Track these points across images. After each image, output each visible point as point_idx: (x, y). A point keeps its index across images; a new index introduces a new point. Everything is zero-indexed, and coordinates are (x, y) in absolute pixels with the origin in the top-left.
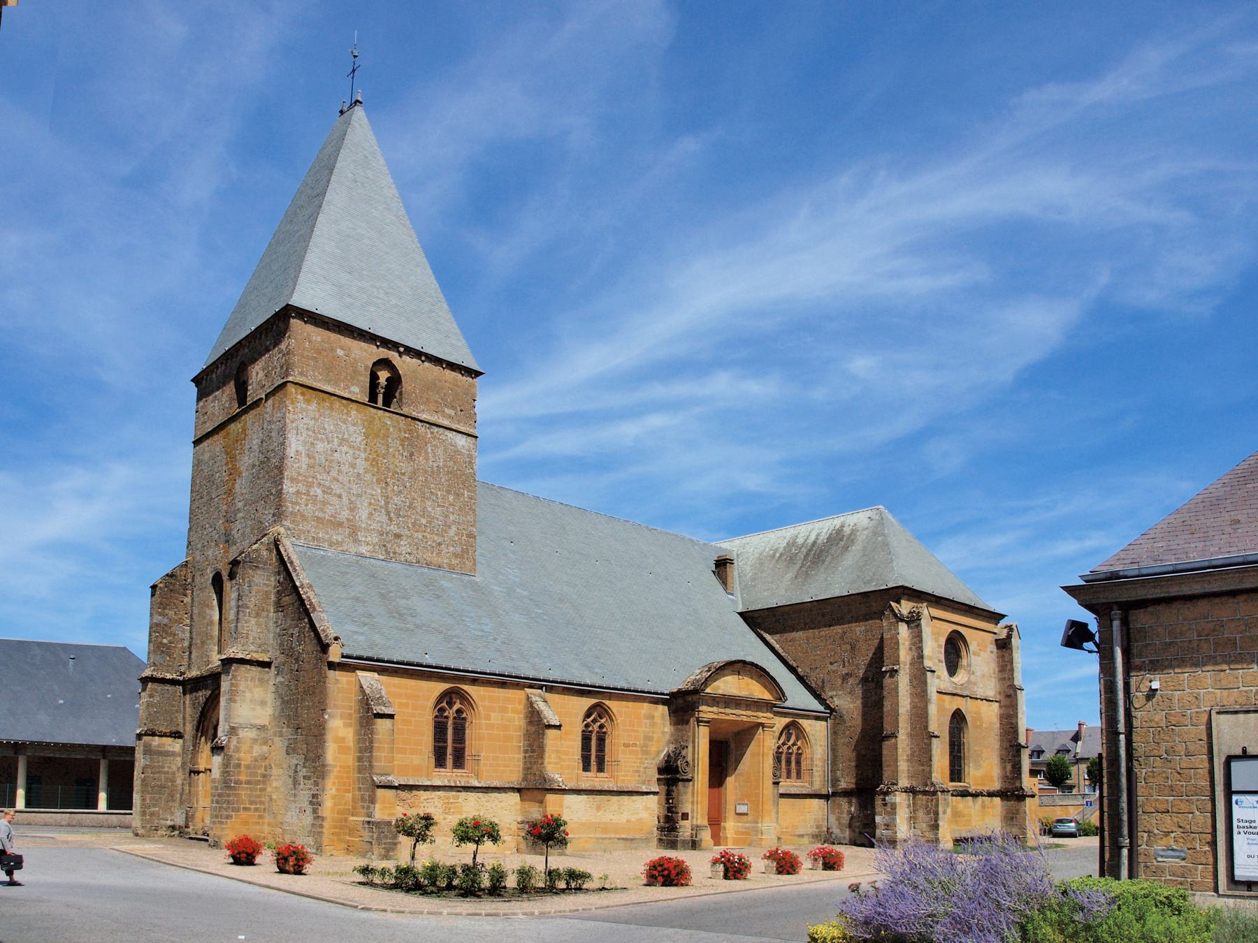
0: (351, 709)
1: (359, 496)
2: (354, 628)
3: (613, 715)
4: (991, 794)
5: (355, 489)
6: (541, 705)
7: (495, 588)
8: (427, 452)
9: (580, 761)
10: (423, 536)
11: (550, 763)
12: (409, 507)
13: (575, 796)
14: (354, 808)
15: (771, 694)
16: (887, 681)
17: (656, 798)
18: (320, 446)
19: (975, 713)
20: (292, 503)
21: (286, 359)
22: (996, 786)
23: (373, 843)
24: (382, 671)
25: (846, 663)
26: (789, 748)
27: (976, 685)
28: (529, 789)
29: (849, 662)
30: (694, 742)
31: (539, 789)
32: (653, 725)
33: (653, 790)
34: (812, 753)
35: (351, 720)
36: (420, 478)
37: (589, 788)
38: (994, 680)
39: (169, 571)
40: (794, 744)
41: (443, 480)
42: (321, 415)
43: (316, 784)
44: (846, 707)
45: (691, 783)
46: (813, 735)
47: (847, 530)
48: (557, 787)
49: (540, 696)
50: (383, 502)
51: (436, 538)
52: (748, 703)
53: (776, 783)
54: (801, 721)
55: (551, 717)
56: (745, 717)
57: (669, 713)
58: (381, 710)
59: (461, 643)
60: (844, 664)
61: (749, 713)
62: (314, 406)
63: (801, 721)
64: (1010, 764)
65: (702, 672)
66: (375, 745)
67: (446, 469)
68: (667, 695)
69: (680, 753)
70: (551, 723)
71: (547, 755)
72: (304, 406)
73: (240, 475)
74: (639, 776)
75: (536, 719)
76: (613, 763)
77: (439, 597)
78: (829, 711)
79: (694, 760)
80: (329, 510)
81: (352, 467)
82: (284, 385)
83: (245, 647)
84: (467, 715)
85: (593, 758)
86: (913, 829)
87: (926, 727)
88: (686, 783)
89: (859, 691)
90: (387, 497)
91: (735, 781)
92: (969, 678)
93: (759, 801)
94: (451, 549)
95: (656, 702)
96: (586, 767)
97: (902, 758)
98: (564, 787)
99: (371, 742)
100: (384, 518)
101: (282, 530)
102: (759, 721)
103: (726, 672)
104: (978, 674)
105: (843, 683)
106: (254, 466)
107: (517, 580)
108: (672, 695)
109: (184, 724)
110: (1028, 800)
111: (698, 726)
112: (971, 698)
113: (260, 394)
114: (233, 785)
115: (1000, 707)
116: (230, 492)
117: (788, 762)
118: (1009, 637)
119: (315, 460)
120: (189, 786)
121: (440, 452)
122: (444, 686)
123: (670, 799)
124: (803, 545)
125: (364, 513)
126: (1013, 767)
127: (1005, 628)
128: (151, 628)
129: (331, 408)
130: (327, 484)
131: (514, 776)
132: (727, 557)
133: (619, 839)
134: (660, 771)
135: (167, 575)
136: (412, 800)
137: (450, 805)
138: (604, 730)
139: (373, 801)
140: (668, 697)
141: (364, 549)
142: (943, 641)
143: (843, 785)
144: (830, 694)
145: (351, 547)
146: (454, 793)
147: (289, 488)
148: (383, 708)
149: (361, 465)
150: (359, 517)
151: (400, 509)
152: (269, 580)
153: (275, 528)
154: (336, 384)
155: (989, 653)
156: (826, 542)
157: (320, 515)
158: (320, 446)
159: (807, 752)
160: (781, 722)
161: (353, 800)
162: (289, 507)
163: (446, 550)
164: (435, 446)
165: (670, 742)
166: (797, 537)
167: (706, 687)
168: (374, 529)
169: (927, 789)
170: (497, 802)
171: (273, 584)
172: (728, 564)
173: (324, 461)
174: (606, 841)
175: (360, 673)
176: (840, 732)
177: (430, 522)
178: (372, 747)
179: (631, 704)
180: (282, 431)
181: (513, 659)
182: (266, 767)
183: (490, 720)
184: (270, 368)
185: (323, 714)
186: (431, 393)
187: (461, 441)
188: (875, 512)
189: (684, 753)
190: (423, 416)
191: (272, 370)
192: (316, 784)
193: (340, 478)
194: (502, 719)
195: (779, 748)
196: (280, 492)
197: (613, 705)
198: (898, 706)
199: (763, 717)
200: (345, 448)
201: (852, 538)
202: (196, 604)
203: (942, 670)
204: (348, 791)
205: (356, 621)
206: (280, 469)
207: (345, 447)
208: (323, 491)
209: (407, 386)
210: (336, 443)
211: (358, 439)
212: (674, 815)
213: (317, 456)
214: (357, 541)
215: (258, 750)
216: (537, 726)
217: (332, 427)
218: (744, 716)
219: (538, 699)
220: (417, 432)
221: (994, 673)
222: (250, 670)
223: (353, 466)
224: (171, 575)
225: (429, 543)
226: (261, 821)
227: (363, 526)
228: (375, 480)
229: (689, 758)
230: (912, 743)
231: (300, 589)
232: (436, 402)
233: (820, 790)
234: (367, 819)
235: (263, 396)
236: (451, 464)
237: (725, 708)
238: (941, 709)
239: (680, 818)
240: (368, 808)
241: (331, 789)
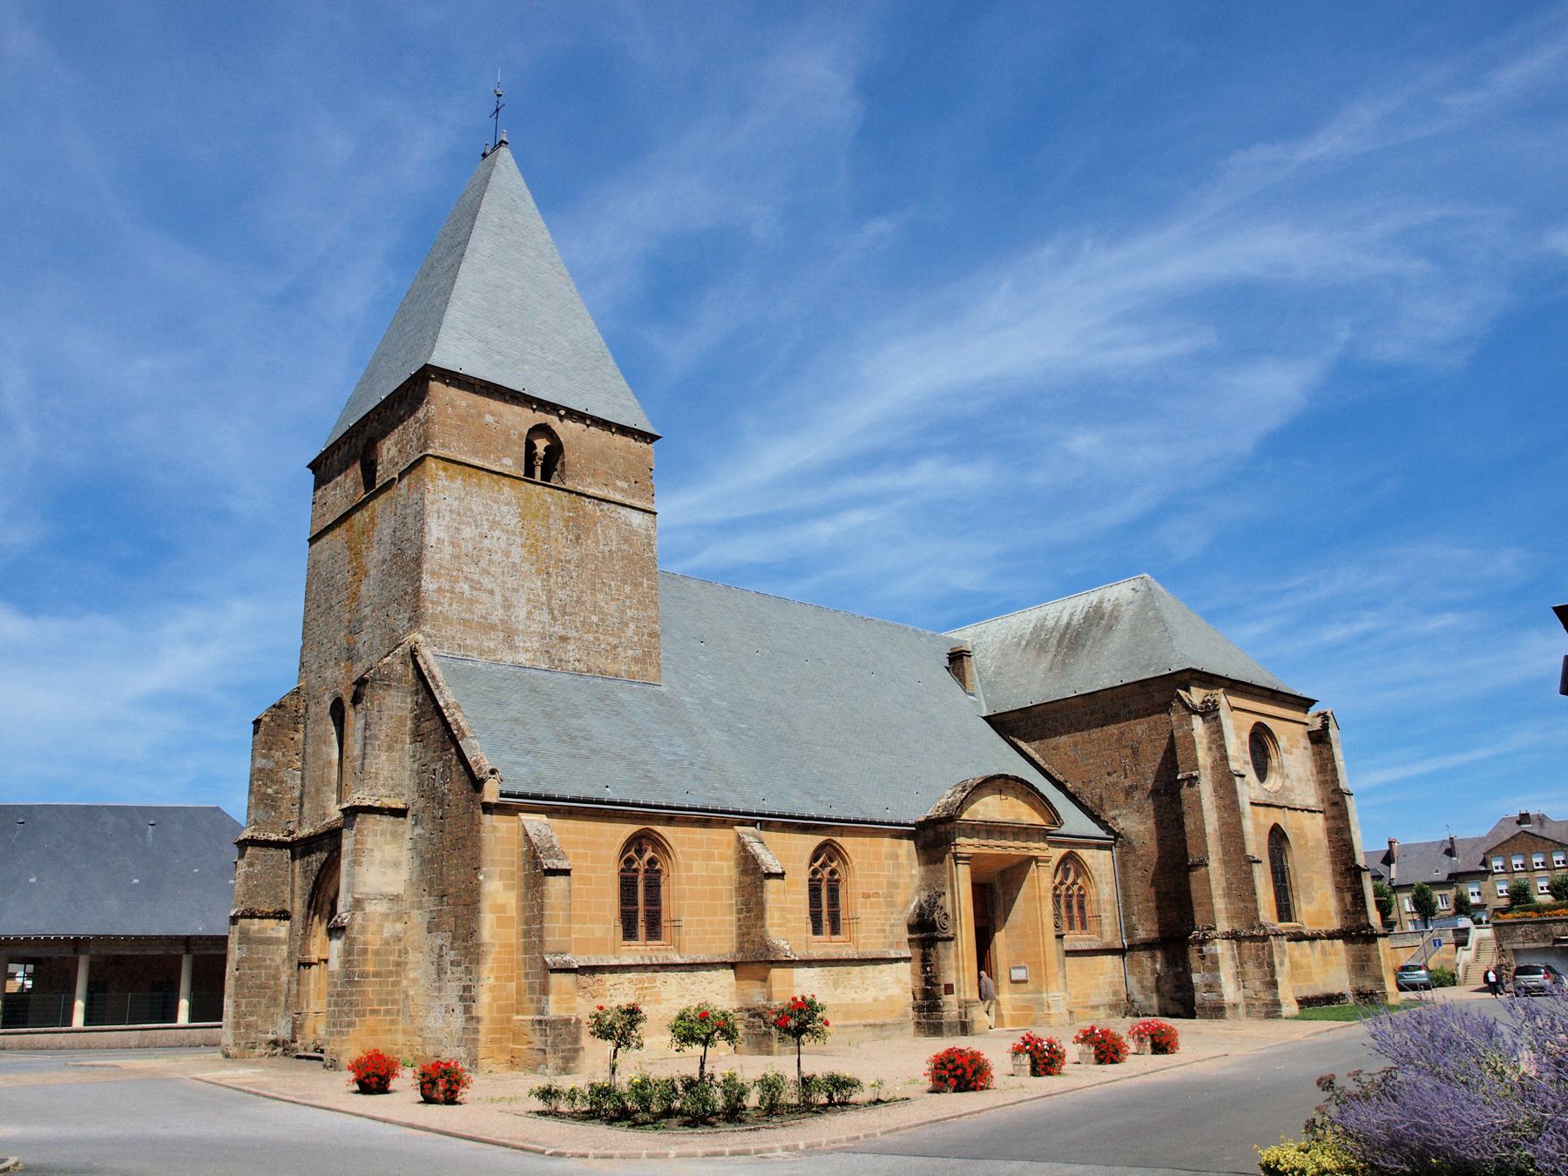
0: (513, 866)
1: (515, 590)
2: (513, 757)
3: (846, 856)
4: (1331, 936)
5: (511, 582)
6: (757, 848)
7: (687, 699)
8: (596, 535)
9: (809, 920)
10: (595, 638)
11: (772, 925)
12: (577, 602)
13: (806, 969)
14: (519, 1002)
15: (1043, 817)
16: (1185, 791)
17: (908, 965)
18: (467, 532)
19: (1297, 829)
20: (432, 602)
21: (424, 430)
22: (1335, 924)
23: (547, 1051)
24: (551, 812)
26: (1068, 888)
27: (1292, 791)
28: (747, 963)
29: (1131, 769)
30: (952, 886)
31: (760, 962)
32: (898, 866)
33: (904, 955)
34: (1098, 894)
35: (513, 880)
36: (589, 566)
37: (823, 957)
38: (1312, 784)
39: (276, 701)
40: (1074, 883)
41: (616, 567)
42: (467, 494)
43: (468, 971)
45: (953, 942)
46: (1096, 870)
47: (1107, 606)
48: (784, 959)
49: (754, 835)
50: (544, 597)
51: (611, 639)
52: (1016, 830)
53: (1060, 937)
54: (1079, 851)
55: (771, 862)
56: (1013, 849)
57: (917, 849)
58: (553, 864)
59: (649, 771)
62: (458, 483)
63: (1079, 851)
64: (1350, 894)
65: (954, 792)
66: (546, 913)
67: (620, 554)
68: (911, 825)
69: (935, 903)
71: (768, 914)
72: (447, 483)
73: (366, 574)
74: (885, 937)
76: (851, 922)
77: (617, 713)
78: (1112, 837)
79: (954, 910)
80: (479, 610)
81: (506, 555)
82: (423, 459)
83: (374, 791)
84: (662, 865)
85: (825, 916)
86: (1242, 989)
87: (1243, 850)
88: (948, 943)
89: (1149, 806)
90: (550, 591)
91: (1007, 937)
92: (1283, 783)
93: (1040, 963)
94: (630, 652)
96: (817, 930)
97: (1217, 893)
98: (792, 957)
99: (542, 909)
100: (546, 617)
101: (420, 637)
102: (1031, 853)
103: (985, 791)
104: (1293, 777)
105: (1126, 798)
106: (384, 561)
107: (712, 688)
108: (919, 825)
109: (292, 900)
110: (1380, 941)
111: (956, 864)
112: (1289, 808)
113: (392, 473)
114: (356, 979)
115: (1326, 819)
116: (354, 596)
117: (1069, 907)
118: (1325, 727)
119: (460, 548)
120: (298, 984)
121: (612, 532)
122: (632, 828)
124: (1054, 629)
125: (521, 613)
126: (1355, 897)
127: (1318, 716)
128: (252, 775)
129: (479, 485)
130: (476, 577)
131: (724, 945)
132: (963, 648)
133: (865, 1026)
134: (912, 928)
135: (274, 706)
136: (596, 987)
137: (645, 991)
138: (836, 877)
139: (545, 990)
140: (914, 829)
141: (522, 658)
142: (1246, 736)
143: (1141, 934)
144: (1112, 813)
145: (506, 656)
146: (649, 974)
147: (429, 584)
148: (556, 861)
149: (517, 553)
150: (516, 617)
151: (566, 605)
152: (406, 703)
153: (411, 637)
154: (485, 457)
155: (1302, 749)
156: (1084, 623)
157: (467, 616)
158: (467, 532)
159: (1091, 893)
160: (1058, 853)
161: (519, 992)
162: (429, 609)
163: (623, 654)
164: (606, 526)
165: (919, 890)
166: (1045, 619)
167: (962, 812)
168: (534, 632)
169: (1254, 933)
170: (705, 984)
171: (410, 706)
172: (965, 657)
173: (471, 549)
174: (850, 1030)
175: (523, 816)
176: (1130, 864)
177: (603, 620)
178: (542, 916)
180: (420, 516)
181: (715, 789)
182: (400, 951)
183: (692, 872)
184: (405, 442)
185: (476, 875)
186: (598, 463)
187: (637, 519)
188: (1139, 583)
189: (940, 902)
190: (591, 491)
191: (407, 443)
192: (468, 971)
193: (492, 570)
194: (707, 869)
195: (1055, 888)
196: (417, 591)
197: (846, 843)
198: (1204, 824)
199: (1036, 848)
200: (497, 533)
201: (1115, 616)
202: (309, 741)
203: (1251, 775)
204: (510, 979)
205: (516, 749)
206: (418, 561)
207: (497, 531)
208: (471, 587)
209: (569, 456)
210: (486, 527)
211: (513, 522)
212: (935, 988)
213: (463, 544)
214: (513, 648)
215: (390, 929)
216: (753, 875)
217: (480, 508)
218: (1013, 848)
219: (752, 839)
220: (583, 510)
221: (1312, 775)
222: (380, 821)
223: (507, 554)
224: (280, 706)
225: (602, 646)
226: (393, 1028)
227: (521, 627)
228: (534, 571)
229: (948, 909)
230: (1227, 873)
231: (445, 711)
232: (606, 473)
234: (539, 1017)
235: (396, 476)
236: (626, 547)
237: (988, 839)
238: (1257, 825)
239: (943, 992)
240: (539, 1001)
241: (488, 977)
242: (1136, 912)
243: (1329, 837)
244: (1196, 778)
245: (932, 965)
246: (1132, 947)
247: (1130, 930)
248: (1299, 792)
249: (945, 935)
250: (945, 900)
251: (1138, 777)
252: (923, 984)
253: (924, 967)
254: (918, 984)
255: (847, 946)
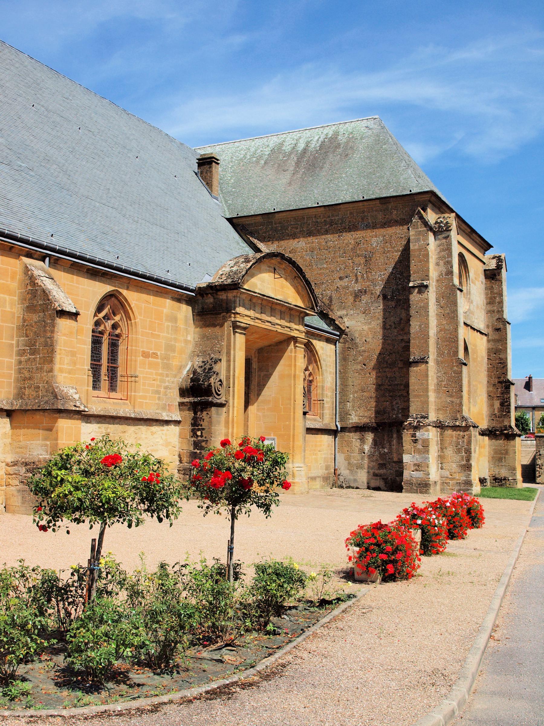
3: (130, 311)
11: (61, 370)
17: (174, 430)
25: (359, 278)
28: (26, 411)
30: (228, 354)
31: (44, 410)
32: (176, 330)
37: (102, 413)
44: (359, 328)
48: (74, 408)
52: (283, 309)
57: (193, 315)
60: (357, 280)
61: (283, 323)
63: (315, 342)
69: (210, 369)
70: (64, 309)
71: (57, 358)
74: (159, 399)
75: (41, 302)
76: (130, 379)
78: (338, 333)
79: (228, 378)
85: (104, 370)
89: (378, 308)
91: (258, 410)
95: (179, 299)
96: (96, 386)
105: (355, 301)
111: (235, 332)
123: (199, 430)
134: (183, 392)
138: (118, 332)
144: (339, 313)
165: (194, 354)
179: (151, 298)
189: (216, 368)
229: (223, 376)
233: (329, 424)
242: (351, 400)
243: (489, 355)
244: (426, 287)
245: (203, 429)
246: (343, 429)
247: (344, 415)
248: (476, 317)
249: (219, 401)
250: (221, 367)
251: (368, 283)
252: (192, 448)
253: (194, 433)
254: (185, 447)
255: (124, 404)
